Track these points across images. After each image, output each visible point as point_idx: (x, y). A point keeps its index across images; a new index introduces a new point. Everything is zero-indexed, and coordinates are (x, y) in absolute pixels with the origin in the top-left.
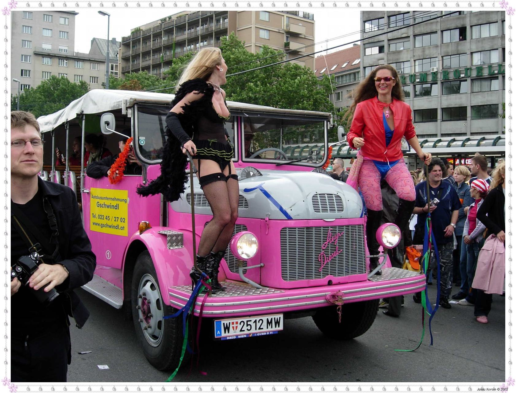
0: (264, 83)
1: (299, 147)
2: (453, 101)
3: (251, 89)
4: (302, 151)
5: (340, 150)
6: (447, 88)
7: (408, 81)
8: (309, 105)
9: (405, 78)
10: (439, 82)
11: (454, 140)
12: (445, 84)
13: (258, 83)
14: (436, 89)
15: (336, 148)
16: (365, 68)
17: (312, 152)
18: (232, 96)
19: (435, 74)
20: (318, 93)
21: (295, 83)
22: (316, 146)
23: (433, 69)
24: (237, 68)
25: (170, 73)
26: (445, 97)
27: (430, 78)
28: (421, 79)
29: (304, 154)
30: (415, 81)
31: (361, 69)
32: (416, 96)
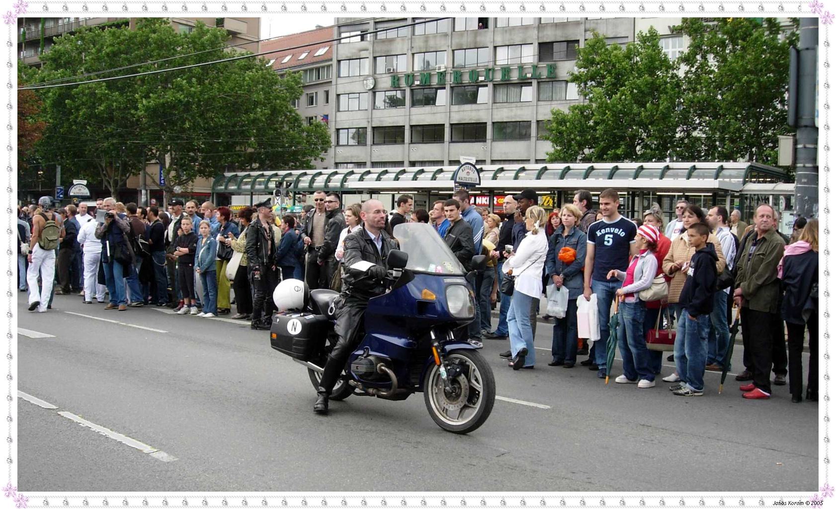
0: (200, 81)
1: (249, 176)
2: (467, 114)
3: (180, 88)
4: (253, 183)
5: (312, 181)
6: (458, 94)
7: (403, 83)
8: (265, 114)
9: (398, 80)
10: (448, 87)
11: (502, 170)
12: (456, 90)
13: (194, 80)
14: (443, 96)
15: (309, 178)
16: (339, 61)
17: (281, 184)
18: (150, 97)
19: (442, 75)
20: (277, 98)
21: (244, 80)
22: (276, 175)
23: (440, 68)
24: (159, 55)
25: (51, 59)
26: (455, 108)
27: (435, 81)
28: (421, 82)
29: (257, 187)
30: (413, 83)
31: (334, 62)
32: (414, 104)
